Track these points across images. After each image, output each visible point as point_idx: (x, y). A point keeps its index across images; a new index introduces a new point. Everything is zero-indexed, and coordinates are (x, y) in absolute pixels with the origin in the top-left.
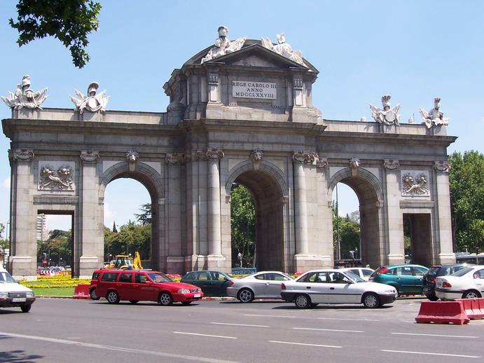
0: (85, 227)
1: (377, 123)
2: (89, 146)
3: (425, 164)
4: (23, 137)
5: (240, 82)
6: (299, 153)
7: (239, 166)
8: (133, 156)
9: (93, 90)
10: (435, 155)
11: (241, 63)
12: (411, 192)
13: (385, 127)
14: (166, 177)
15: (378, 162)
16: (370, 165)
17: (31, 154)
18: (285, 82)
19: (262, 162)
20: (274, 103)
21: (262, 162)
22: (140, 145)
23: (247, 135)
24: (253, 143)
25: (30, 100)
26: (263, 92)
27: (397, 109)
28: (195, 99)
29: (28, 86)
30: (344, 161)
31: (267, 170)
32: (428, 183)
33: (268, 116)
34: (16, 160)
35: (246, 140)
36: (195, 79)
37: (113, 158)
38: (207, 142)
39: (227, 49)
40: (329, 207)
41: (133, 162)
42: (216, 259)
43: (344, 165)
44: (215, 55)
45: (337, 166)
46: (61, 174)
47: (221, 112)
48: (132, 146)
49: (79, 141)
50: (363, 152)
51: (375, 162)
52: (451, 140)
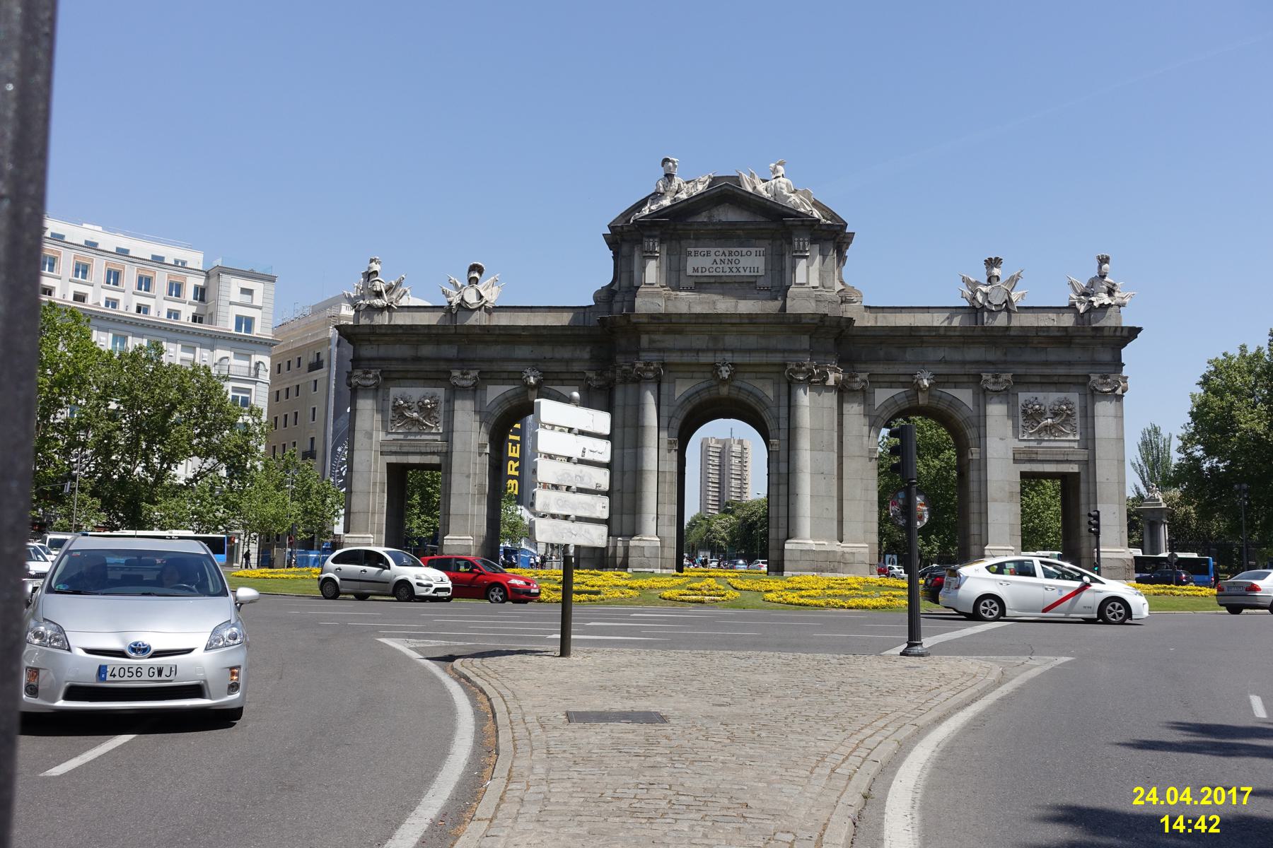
0: (454, 490)
2: (464, 363)
3: (1070, 380)
4: (368, 351)
5: (700, 250)
7: (695, 391)
8: (532, 378)
9: (476, 275)
10: (1094, 363)
11: (703, 218)
12: (1039, 432)
13: (986, 314)
16: (956, 385)
18: (781, 245)
19: (738, 383)
21: (738, 383)
22: (545, 360)
25: (379, 295)
27: (1013, 280)
29: (376, 272)
30: (902, 379)
31: (743, 396)
32: (1077, 415)
33: (747, 306)
35: (704, 347)
37: (504, 381)
38: (637, 352)
39: (678, 195)
40: (871, 459)
42: (642, 544)
43: (903, 384)
44: (653, 207)
45: (891, 387)
46: (422, 408)
47: (662, 302)
48: (533, 360)
50: (940, 362)
51: (965, 379)
52: (1125, 333)
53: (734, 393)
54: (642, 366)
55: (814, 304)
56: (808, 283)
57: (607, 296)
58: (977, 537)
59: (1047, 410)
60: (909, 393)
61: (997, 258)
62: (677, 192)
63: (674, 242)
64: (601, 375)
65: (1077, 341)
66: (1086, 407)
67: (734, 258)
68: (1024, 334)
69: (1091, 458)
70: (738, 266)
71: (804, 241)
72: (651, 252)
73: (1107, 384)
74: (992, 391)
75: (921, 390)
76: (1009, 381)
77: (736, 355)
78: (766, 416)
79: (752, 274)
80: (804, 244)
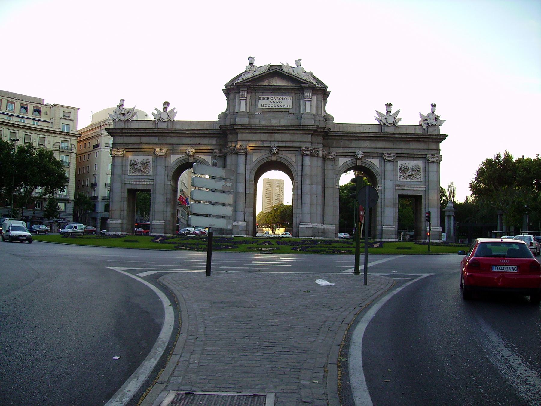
1: (380, 124)
4: (119, 140)
5: (264, 97)
7: (262, 158)
9: (166, 106)
11: (266, 83)
16: (373, 157)
18: (300, 95)
20: (290, 111)
21: (279, 155)
23: (267, 135)
24: (271, 141)
26: (282, 104)
27: (398, 112)
30: (350, 154)
32: (422, 172)
34: (114, 156)
35: (266, 140)
44: (243, 78)
48: (191, 144)
51: (376, 155)
52: (441, 137)
53: (279, 160)
54: (239, 147)
56: (311, 112)
57: (223, 116)
58: (380, 222)
59: (410, 169)
60: (353, 161)
61: (390, 104)
62: (255, 71)
63: (253, 94)
64: (221, 151)
65: (422, 140)
67: (279, 101)
68: (401, 136)
71: (309, 94)
72: (243, 97)
73: (434, 158)
74: (387, 160)
75: (359, 159)
76: (394, 156)
77: (279, 142)
78: (292, 169)
79: (287, 108)
80: (309, 95)
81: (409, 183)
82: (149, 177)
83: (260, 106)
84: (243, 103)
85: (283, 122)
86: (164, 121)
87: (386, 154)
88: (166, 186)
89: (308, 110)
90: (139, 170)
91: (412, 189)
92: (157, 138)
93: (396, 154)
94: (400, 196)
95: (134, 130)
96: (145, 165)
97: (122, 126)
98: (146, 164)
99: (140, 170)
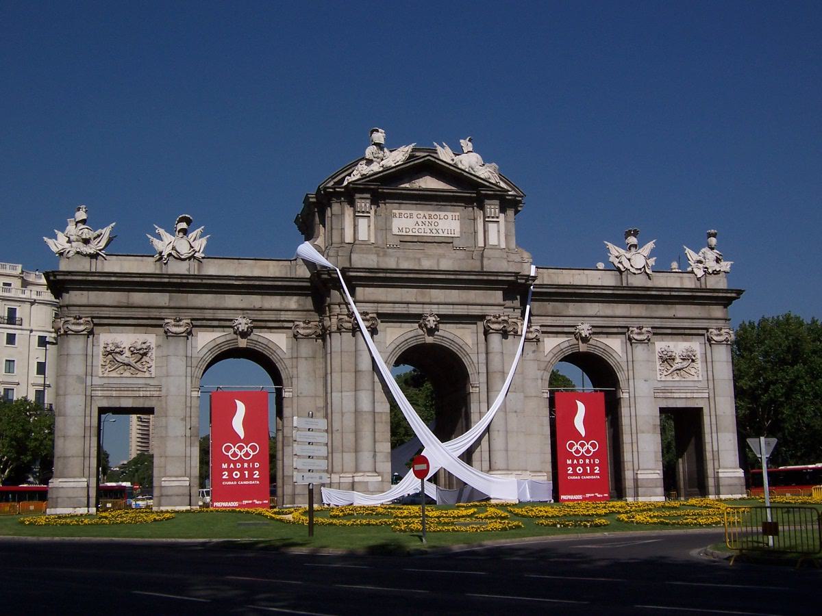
6: (494, 317)
9: (184, 225)
13: (629, 276)
14: (295, 355)
15: (620, 330)
17: (87, 323)
20: (456, 243)
26: (439, 227)
28: (336, 239)
30: (566, 330)
35: (414, 300)
36: (336, 207)
39: (382, 163)
41: (244, 335)
42: (366, 479)
49: (164, 305)
51: (615, 330)
52: (733, 295)
55: (506, 263)
56: (499, 245)
59: (677, 356)
60: (572, 343)
62: (382, 160)
66: (706, 354)
67: (434, 220)
69: (712, 395)
70: (437, 228)
72: (363, 212)
73: (721, 335)
74: (636, 340)
79: (450, 235)
81: (677, 384)
82: (152, 382)
83: (395, 231)
84: (363, 223)
85: (446, 265)
86: (183, 257)
87: (633, 329)
88: (189, 399)
89: (493, 240)
90: (125, 364)
91: (683, 395)
92: (168, 294)
93: (652, 328)
94: (662, 410)
95: (117, 277)
96: (142, 353)
97: (84, 265)
98: (141, 352)
99: (129, 365)
